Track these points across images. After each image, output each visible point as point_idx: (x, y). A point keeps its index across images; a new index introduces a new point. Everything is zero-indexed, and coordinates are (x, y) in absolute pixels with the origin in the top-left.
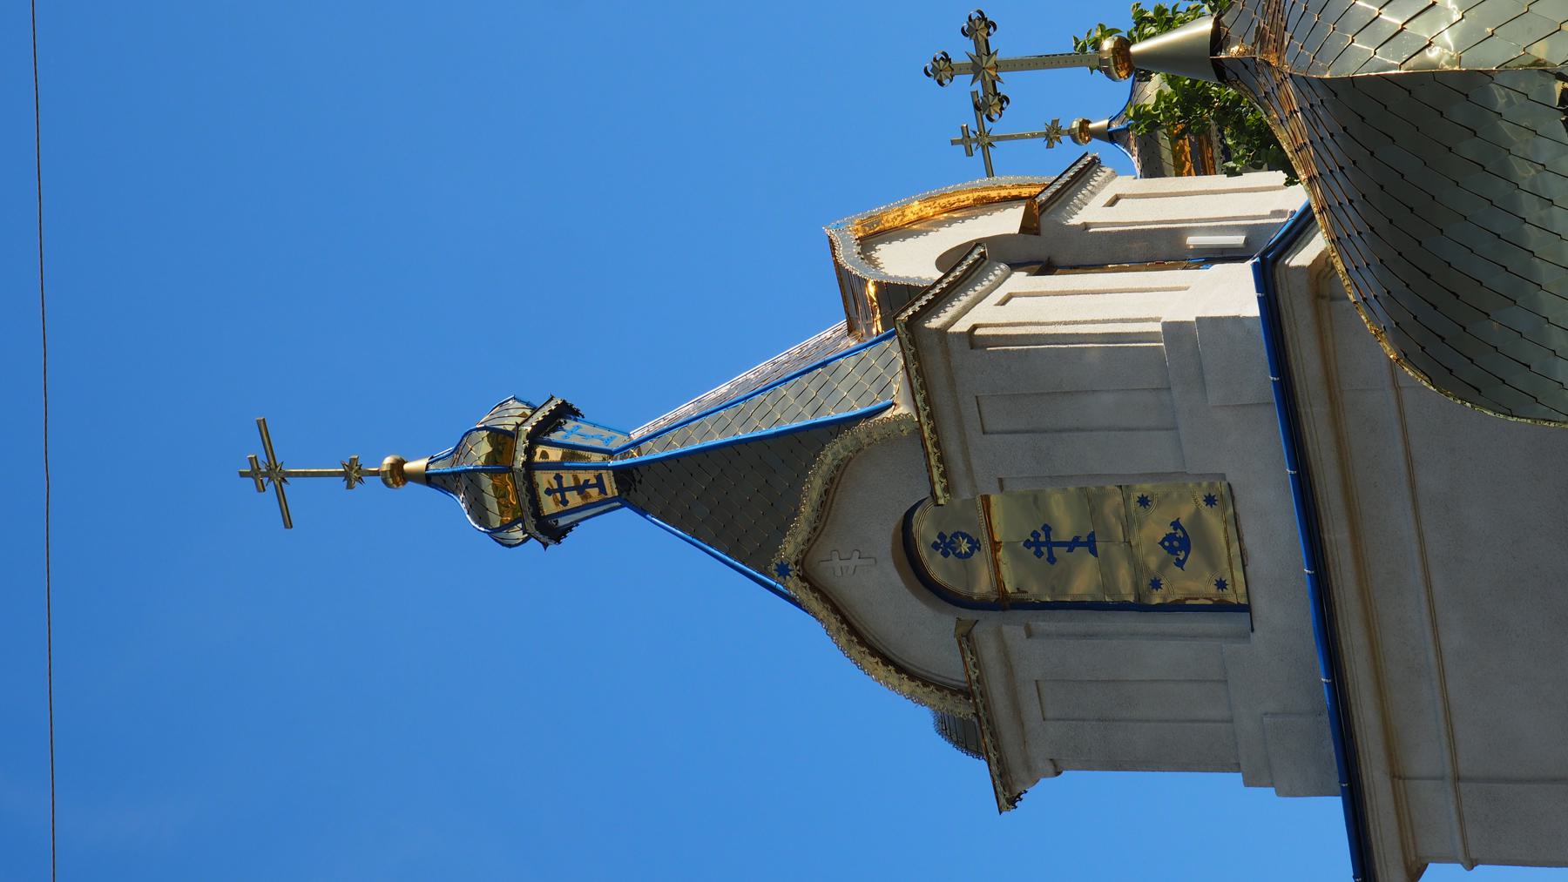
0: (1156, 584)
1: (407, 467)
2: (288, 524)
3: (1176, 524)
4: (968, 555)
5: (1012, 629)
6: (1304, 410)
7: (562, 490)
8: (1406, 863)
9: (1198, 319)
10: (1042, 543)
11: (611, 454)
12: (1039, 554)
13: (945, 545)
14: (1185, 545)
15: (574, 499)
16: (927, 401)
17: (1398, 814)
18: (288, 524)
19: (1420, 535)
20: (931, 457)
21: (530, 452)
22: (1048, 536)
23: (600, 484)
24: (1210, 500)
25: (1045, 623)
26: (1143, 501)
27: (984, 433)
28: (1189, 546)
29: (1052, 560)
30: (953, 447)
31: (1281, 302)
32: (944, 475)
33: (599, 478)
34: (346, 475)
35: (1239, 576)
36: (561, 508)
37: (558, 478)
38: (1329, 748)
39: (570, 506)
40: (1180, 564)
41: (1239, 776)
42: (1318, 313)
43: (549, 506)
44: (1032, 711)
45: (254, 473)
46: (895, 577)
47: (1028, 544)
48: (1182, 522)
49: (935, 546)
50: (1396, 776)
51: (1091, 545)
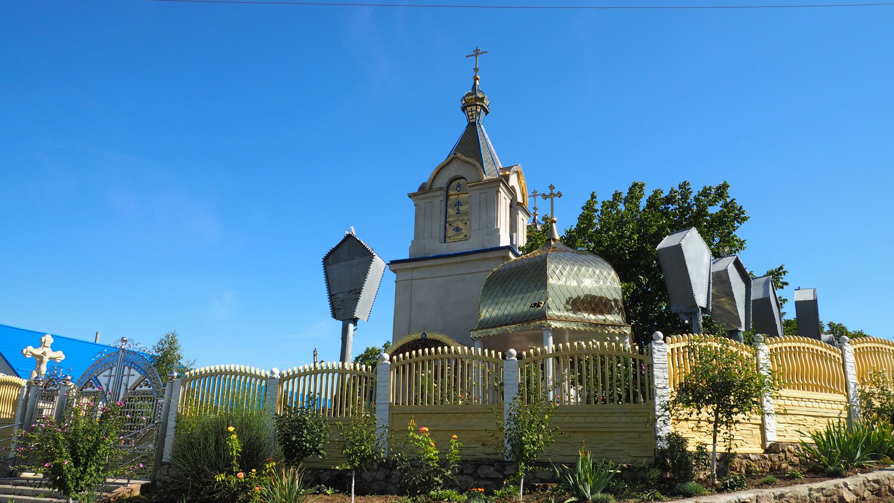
2: (467, 57)
5: (442, 198)
7: (472, 111)
10: (458, 204)
11: (478, 121)
12: (456, 203)
13: (459, 185)
14: (457, 231)
15: (470, 114)
16: (486, 183)
18: (467, 57)
21: (479, 105)
23: (473, 119)
24: (466, 236)
25: (444, 203)
26: (466, 223)
29: (455, 205)
30: (477, 187)
32: (472, 185)
34: (476, 68)
35: (451, 241)
37: (474, 111)
38: (418, 256)
40: (454, 230)
41: (413, 239)
43: (469, 109)
44: (427, 201)
45: (477, 50)
49: (459, 183)
50: (413, 269)
51: (458, 213)
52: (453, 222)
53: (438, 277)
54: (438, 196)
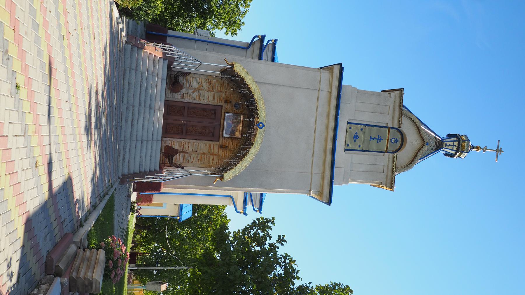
0: (362, 129)
1: (476, 149)
2: (499, 141)
3: (355, 141)
4: (393, 139)
5: (390, 125)
6: (329, 173)
7: (453, 146)
8: (333, 74)
9: (342, 185)
10: (379, 139)
12: (380, 137)
13: (396, 141)
17: (332, 84)
18: (499, 141)
19: (314, 143)
20: (395, 161)
21: (456, 154)
22: (378, 141)
23: (446, 145)
27: (384, 165)
28: (354, 136)
29: (378, 136)
30: (391, 164)
31: (328, 195)
33: (446, 146)
34: (486, 149)
36: (454, 142)
37: (453, 148)
39: (453, 142)
40: (356, 133)
41: (358, 89)
42: (322, 191)
43: (456, 143)
44: (391, 108)
46: (407, 138)
47: (382, 140)
48: (354, 141)
49: (398, 141)
50: (330, 93)
52: (364, 133)
53: (316, 121)
54: (393, 122)
